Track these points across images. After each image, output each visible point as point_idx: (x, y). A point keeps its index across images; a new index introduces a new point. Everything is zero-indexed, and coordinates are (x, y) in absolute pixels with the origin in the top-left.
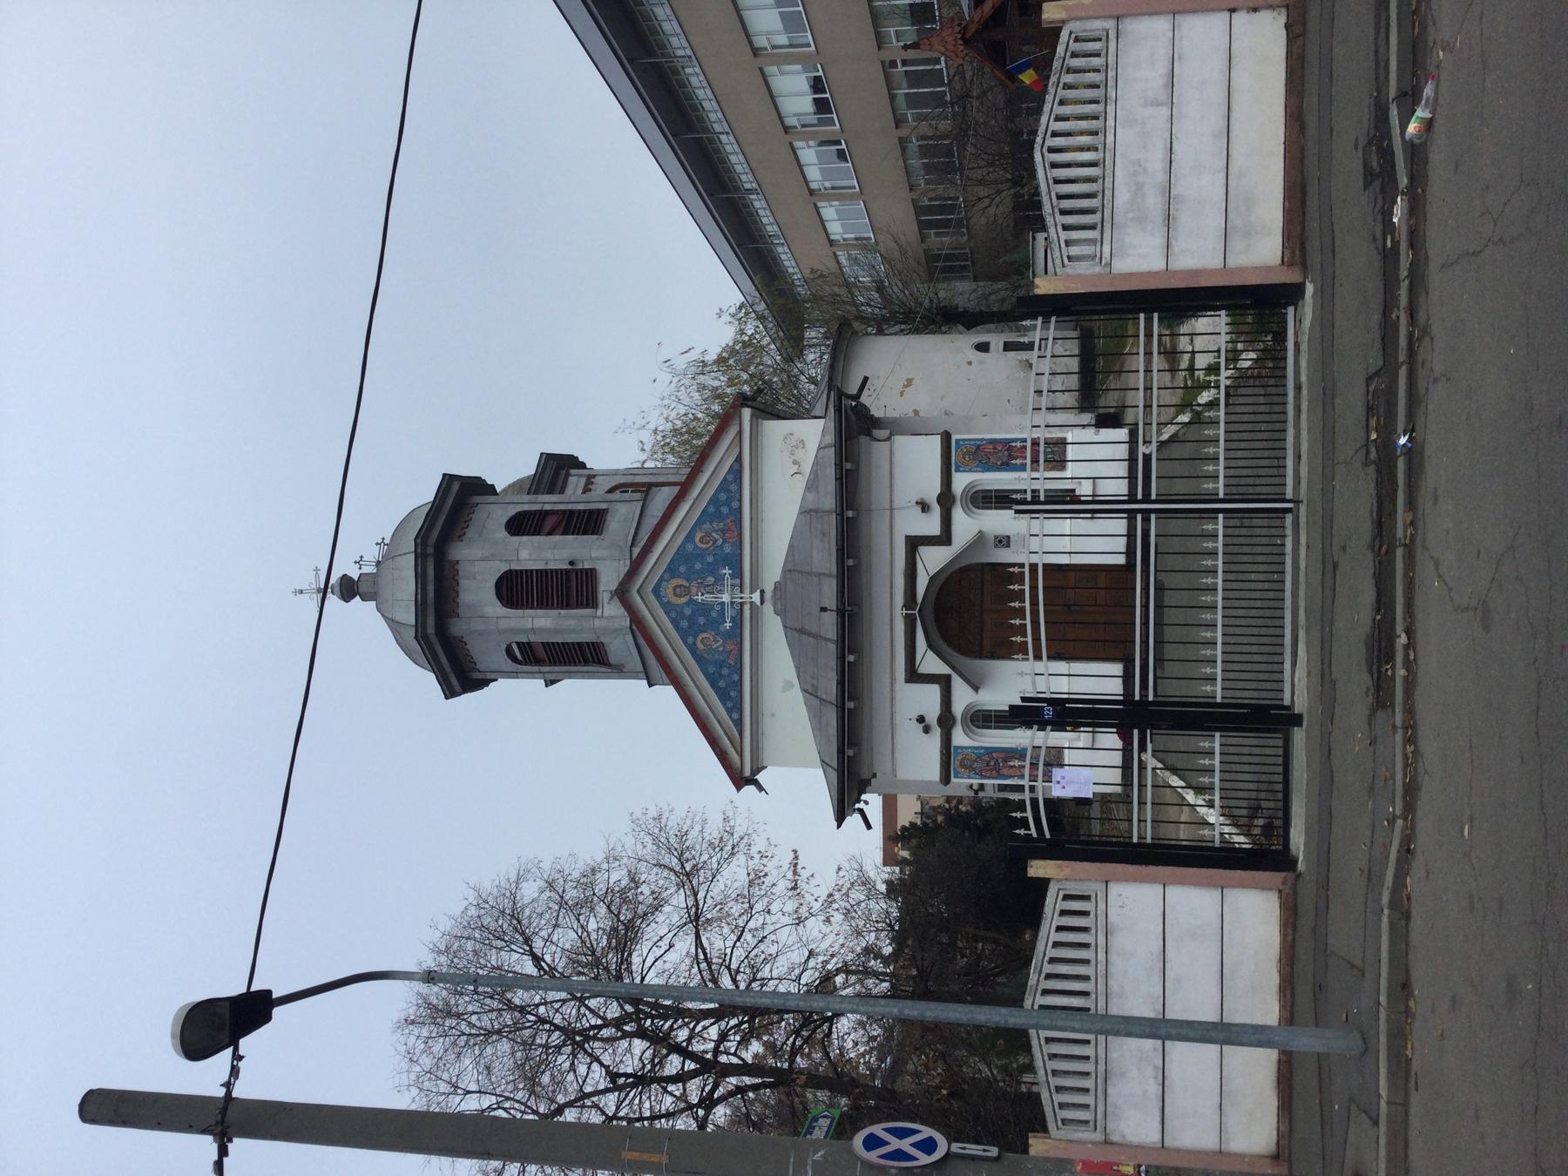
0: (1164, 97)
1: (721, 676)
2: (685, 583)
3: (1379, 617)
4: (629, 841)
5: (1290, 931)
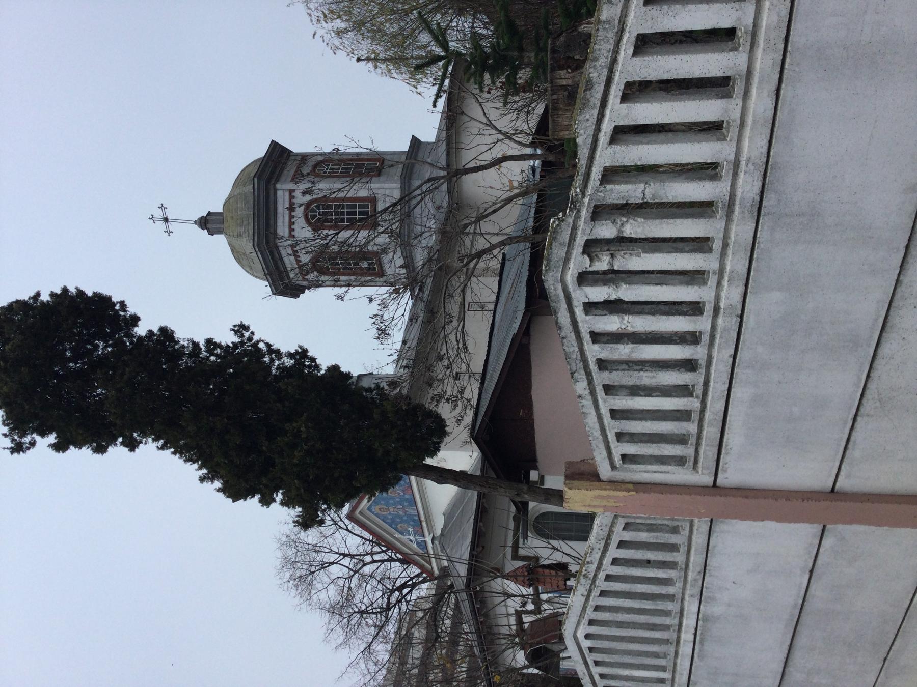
2: (385, 507)
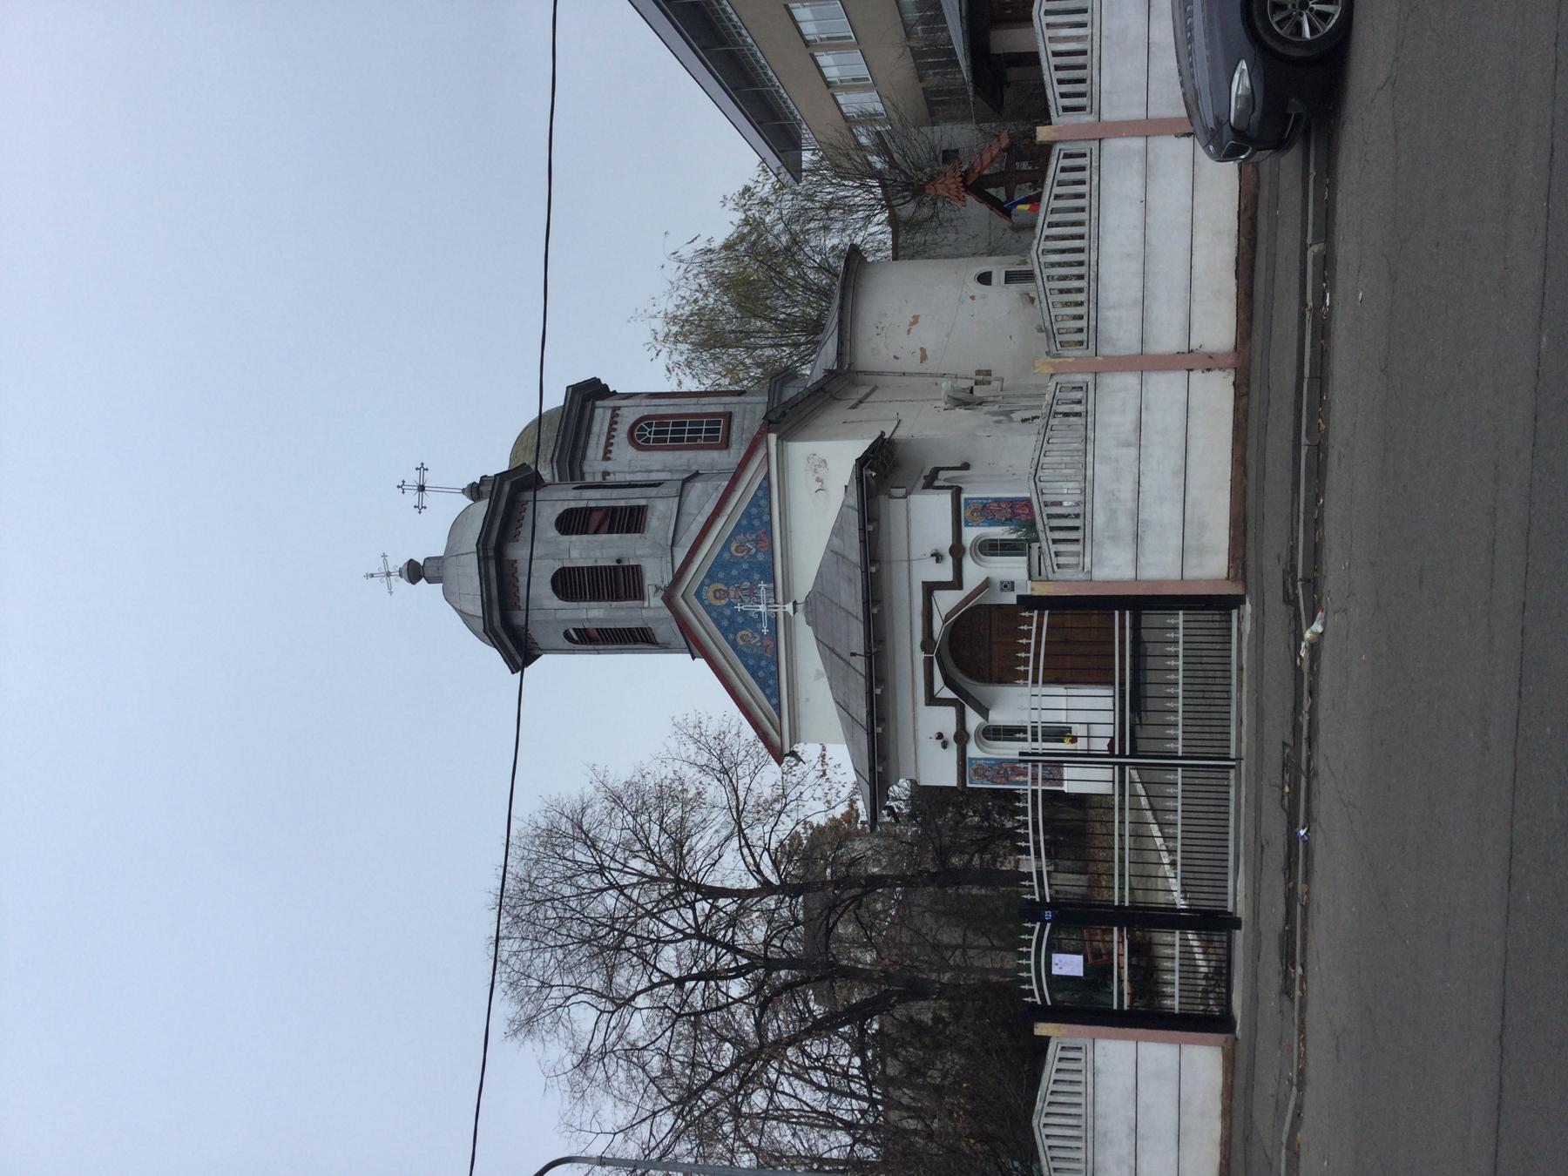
0: (1133, 439)
1: (761, 668)
3: (1287, 928)
4: (673, 744)
5: (1230, 1075)
